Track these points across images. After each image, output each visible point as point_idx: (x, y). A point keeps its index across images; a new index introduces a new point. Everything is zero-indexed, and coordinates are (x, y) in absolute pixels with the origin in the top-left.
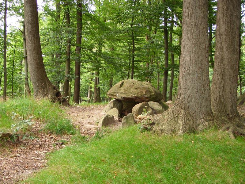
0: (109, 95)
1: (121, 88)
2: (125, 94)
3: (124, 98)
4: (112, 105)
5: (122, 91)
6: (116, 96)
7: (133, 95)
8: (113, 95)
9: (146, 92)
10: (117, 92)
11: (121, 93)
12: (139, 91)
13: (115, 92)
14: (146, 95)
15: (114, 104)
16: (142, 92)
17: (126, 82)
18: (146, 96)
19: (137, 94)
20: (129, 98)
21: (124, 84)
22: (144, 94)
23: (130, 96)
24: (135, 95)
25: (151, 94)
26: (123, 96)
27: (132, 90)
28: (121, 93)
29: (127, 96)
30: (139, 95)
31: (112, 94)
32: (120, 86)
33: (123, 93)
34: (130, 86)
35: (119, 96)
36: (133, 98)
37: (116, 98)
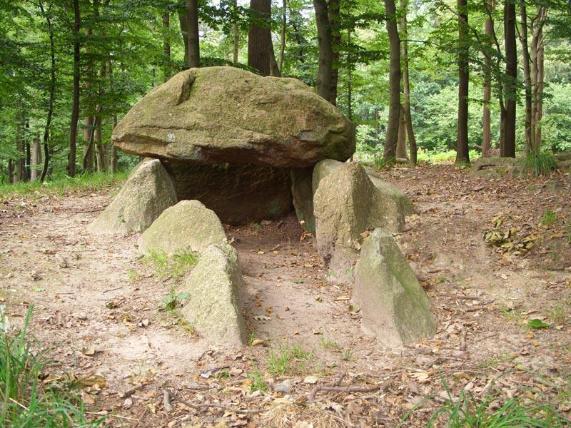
0: (123, 140)
1: (185, 105)
2: (212, 130)
3: (205, 149)
4: (150, 186)
5: (191, 118)
6: (165, 144)
7: (258, 136)
8: (148, 141)
9: (308, 120)
10: (167, 124)
11: (189, 129)
12: (278, 114)
13: (159, 123)
14: (311, 134)
15: (157, 181)
16: (293, 118)
17: (205, 77)
18: (310, 137)
19: (274, 127)
20: (218, 149)
21: (199, 84)
22: (304, 126)
23: (241, 141)
24: (266, 136)
25: (329, 128)
26: (202, 139)
27: (246, 112)
28: (189, 129)
29: (220, 141)
30: (283, 136)
31: (144, 134)
32: (182, 96)
33: (202, 129)
34: (229, 95)
35: (183, 144)
36: (253, 149)
37: (161, 151)
